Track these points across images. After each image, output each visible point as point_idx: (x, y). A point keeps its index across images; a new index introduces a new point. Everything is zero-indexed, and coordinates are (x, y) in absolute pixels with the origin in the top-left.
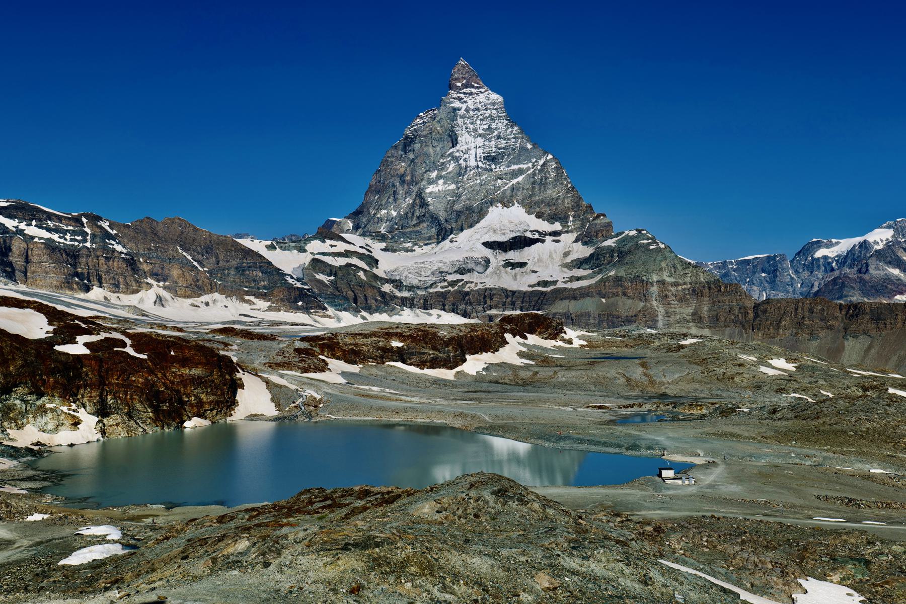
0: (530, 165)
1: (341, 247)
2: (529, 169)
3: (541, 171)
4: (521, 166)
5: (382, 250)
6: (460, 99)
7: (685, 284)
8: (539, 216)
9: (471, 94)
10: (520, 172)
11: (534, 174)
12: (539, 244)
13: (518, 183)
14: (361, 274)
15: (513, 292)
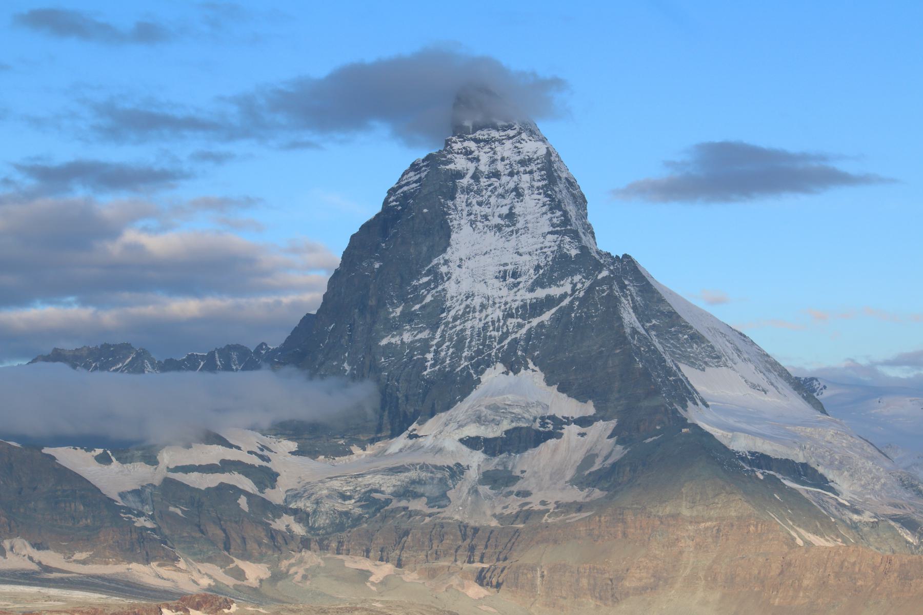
0: (568, 288)
1: (214, 454)
2: (564, 296)
3: (583, 301)
4: (555, 291)
5: (293, 453)
6: (467, 153)
7: (710, 519)
8: (561, 389)
9: (487, 142)
10: (550, 302)
11: (570, 306)
12: (551, 442)
13: (541, 325)
14: (243, 501)
15: (476, 530)
